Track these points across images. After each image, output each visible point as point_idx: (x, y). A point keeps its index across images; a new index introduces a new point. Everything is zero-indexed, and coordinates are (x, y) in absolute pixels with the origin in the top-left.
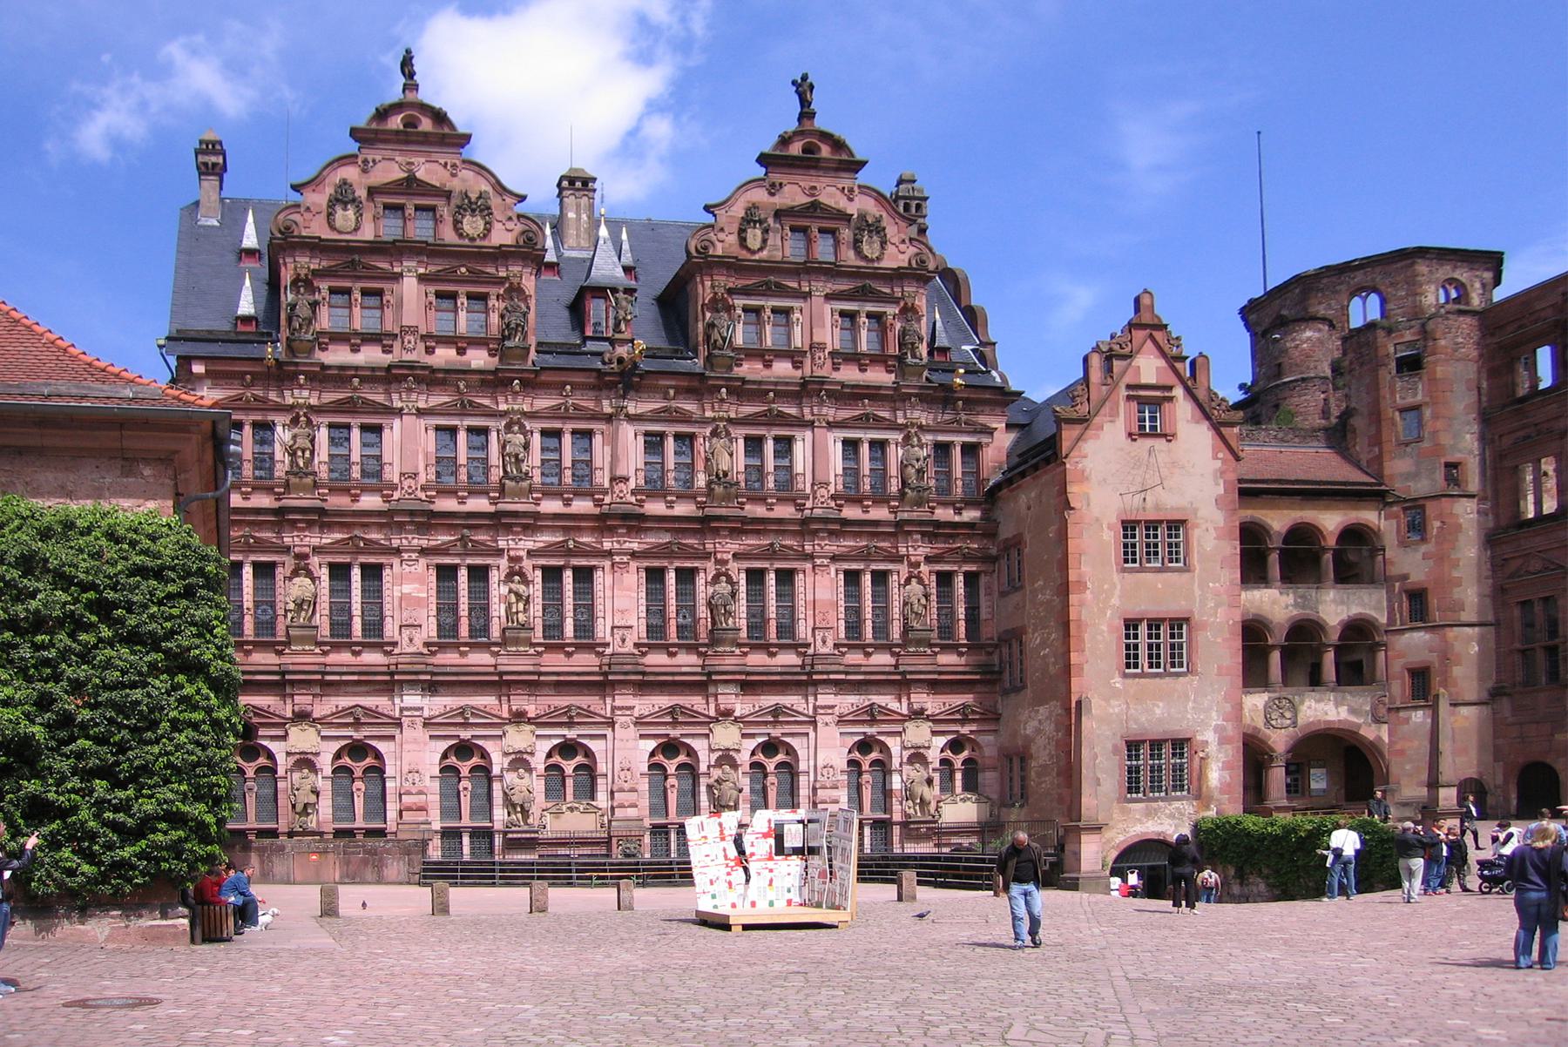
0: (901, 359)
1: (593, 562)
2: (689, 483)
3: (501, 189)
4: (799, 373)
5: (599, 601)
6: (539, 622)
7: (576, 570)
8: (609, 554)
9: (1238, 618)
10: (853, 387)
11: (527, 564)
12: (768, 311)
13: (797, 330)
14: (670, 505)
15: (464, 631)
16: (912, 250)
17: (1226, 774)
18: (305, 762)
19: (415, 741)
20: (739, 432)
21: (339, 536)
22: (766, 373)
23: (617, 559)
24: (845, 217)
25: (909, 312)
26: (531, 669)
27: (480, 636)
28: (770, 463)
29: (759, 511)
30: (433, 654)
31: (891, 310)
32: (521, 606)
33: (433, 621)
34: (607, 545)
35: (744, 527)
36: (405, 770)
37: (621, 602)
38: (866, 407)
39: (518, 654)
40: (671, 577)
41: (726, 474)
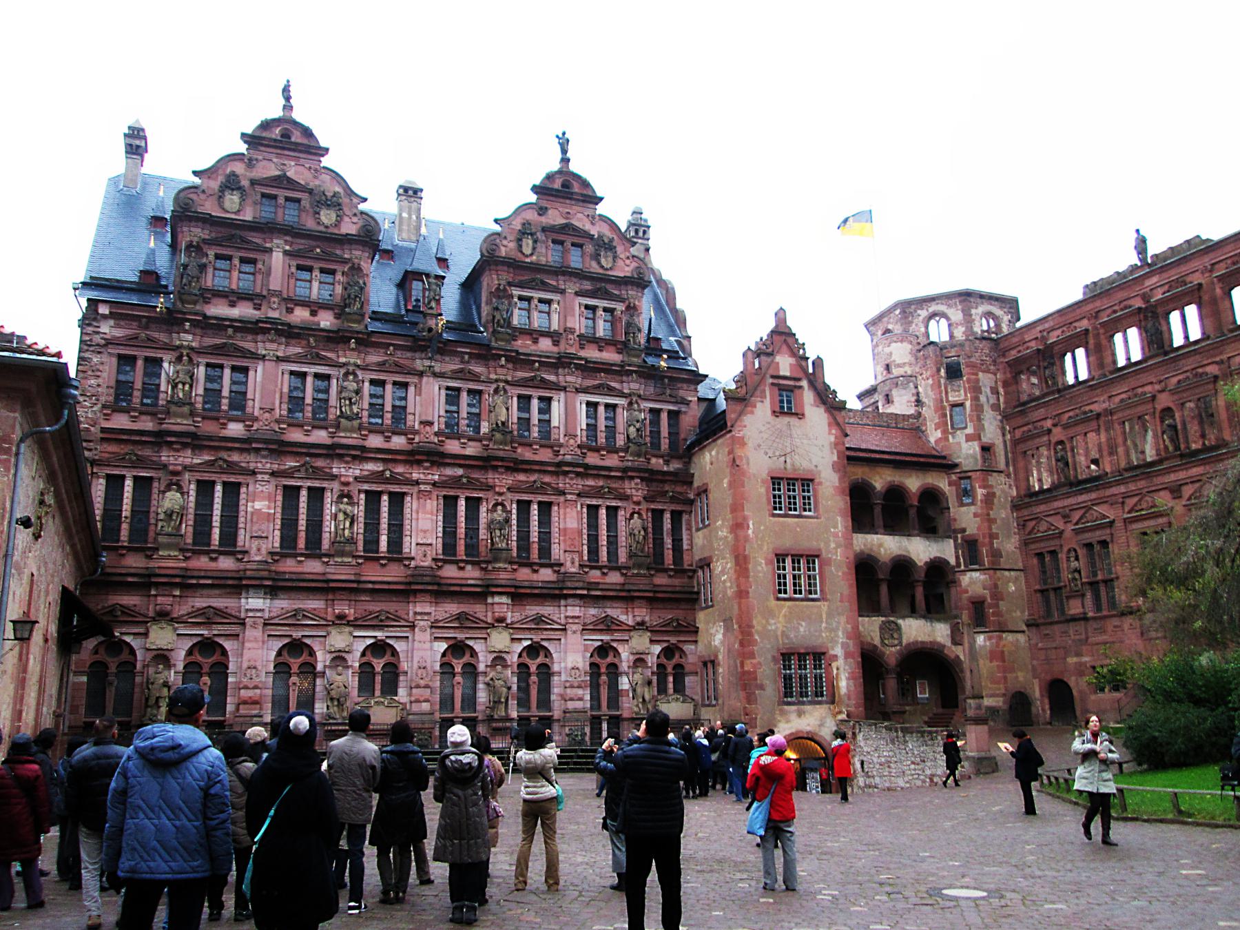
0: (625, 344)
1: (404, 489)
2: (477, 429)
3: (350, 193)
4: (555, 349)
5: (407, 522)
6: (361, 537)
7: (391, 494)
8: (417, 483)
9: (852, 557)
10: (595, 363)
11: (354, 489)
12: (536, 301)
13: (555, 317)
14: (464, 446)
15: (301, 543)
16: (634, 265)
17: (851, 683)
18: (162, 658)
19: (256, 640)
20: (514, 391)
21: (207, 458)
22: (533, 347)
23: (422, 487)
24: (591, 237)
25: (632, 309)
26: (352, 578)
27: (314, 548)
28: (535, 416)
29: (527, 454)
30: (277, 561)
31: (620, 307)
32: (347, 524)
33: (277, 533)
34: (415, 476)
35: (516, 466)
36: (245, 665)
37: (424, 525)
38: (602, 378)
39: (343, 564)
40: (462, 503)
41: (503, 423)
